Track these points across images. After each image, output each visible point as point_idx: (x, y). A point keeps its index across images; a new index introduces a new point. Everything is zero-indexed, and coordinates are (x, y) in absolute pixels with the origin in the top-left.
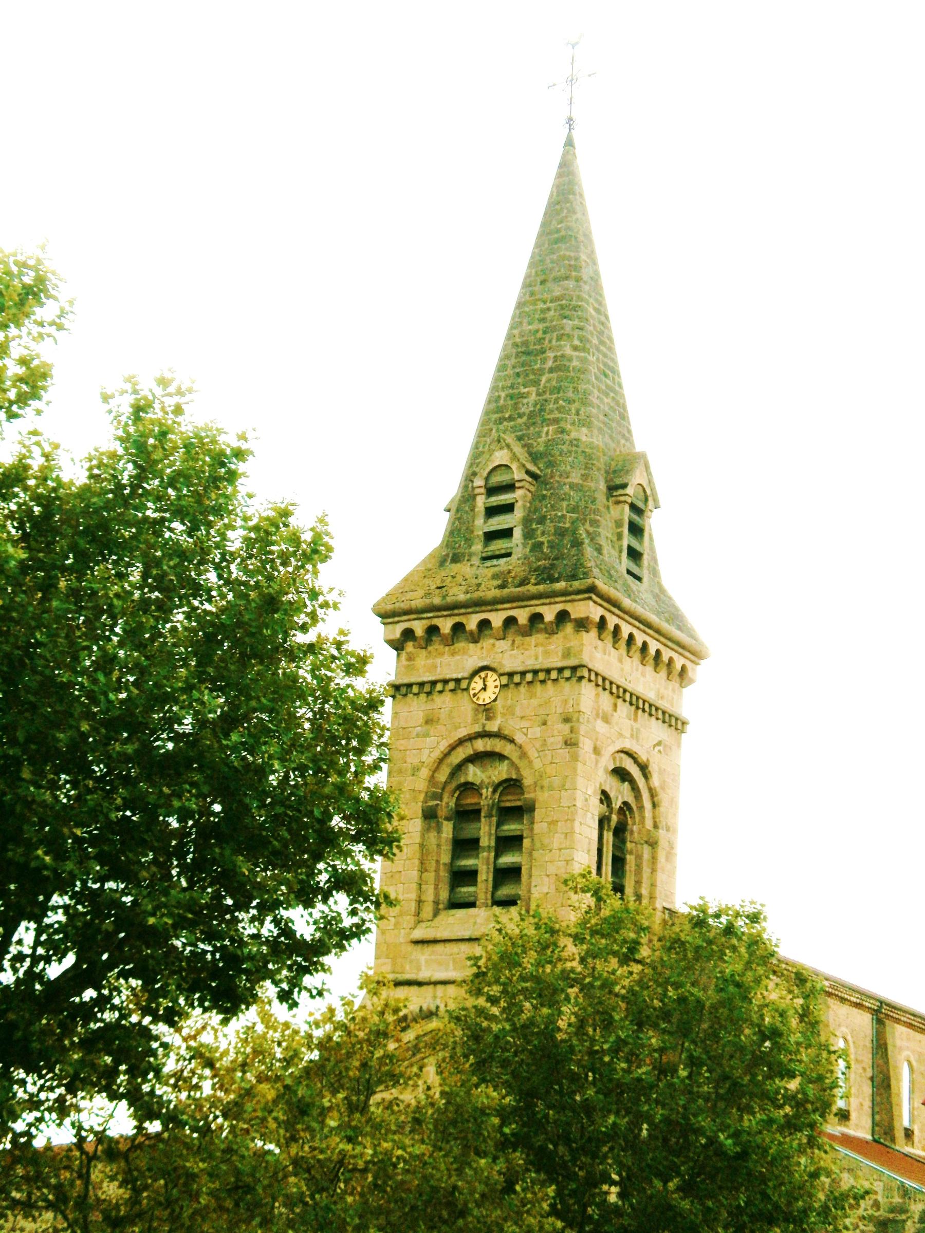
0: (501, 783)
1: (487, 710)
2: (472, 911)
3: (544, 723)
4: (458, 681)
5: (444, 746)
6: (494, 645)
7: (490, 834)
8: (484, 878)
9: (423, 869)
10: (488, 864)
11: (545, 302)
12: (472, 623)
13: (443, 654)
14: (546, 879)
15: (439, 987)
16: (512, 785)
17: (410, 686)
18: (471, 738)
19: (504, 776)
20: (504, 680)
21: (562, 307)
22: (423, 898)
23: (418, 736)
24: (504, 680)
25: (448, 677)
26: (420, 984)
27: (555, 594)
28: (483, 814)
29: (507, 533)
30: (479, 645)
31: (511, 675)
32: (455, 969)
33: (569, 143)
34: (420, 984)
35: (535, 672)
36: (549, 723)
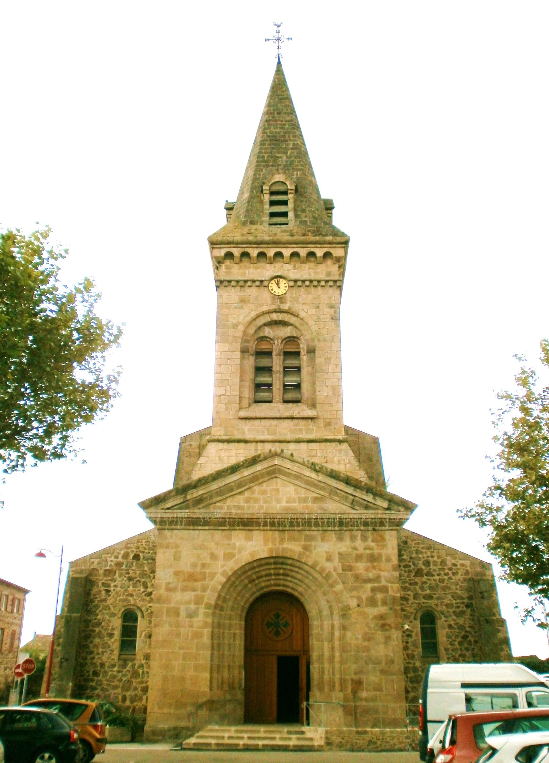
0: (285, 339)
1: (281, 298)
2: (271, 404)
3: (318, 307)
4: (262, 281)
5: (253, 314)
6: (282, 266)
7: (280, 365)
8: (278, 387)
9: (241, 380)
10: (279, 380)
11: (282, 121)
12: (271, 252)
13: (250, 267)
14: (326, 388)
15: (259, 444)
16: (292, 340)
17: (230, 281)
18: (269, 312)
19: (289, 335)
20: (292, 284)
21: (292, 125)
22: (242, 396)
23: (236, 308)
24: (292, 284)
25: (255, 279)
26: (246, 442)
27: (325, 243)
28: (274, 353)
29: (285, 214)
30: (273, 265)
31: (296, 281)
32: (268, 435)
33: (279, 63)
34: (246, 442)
35: (311, 281)
36: (321, 308)
